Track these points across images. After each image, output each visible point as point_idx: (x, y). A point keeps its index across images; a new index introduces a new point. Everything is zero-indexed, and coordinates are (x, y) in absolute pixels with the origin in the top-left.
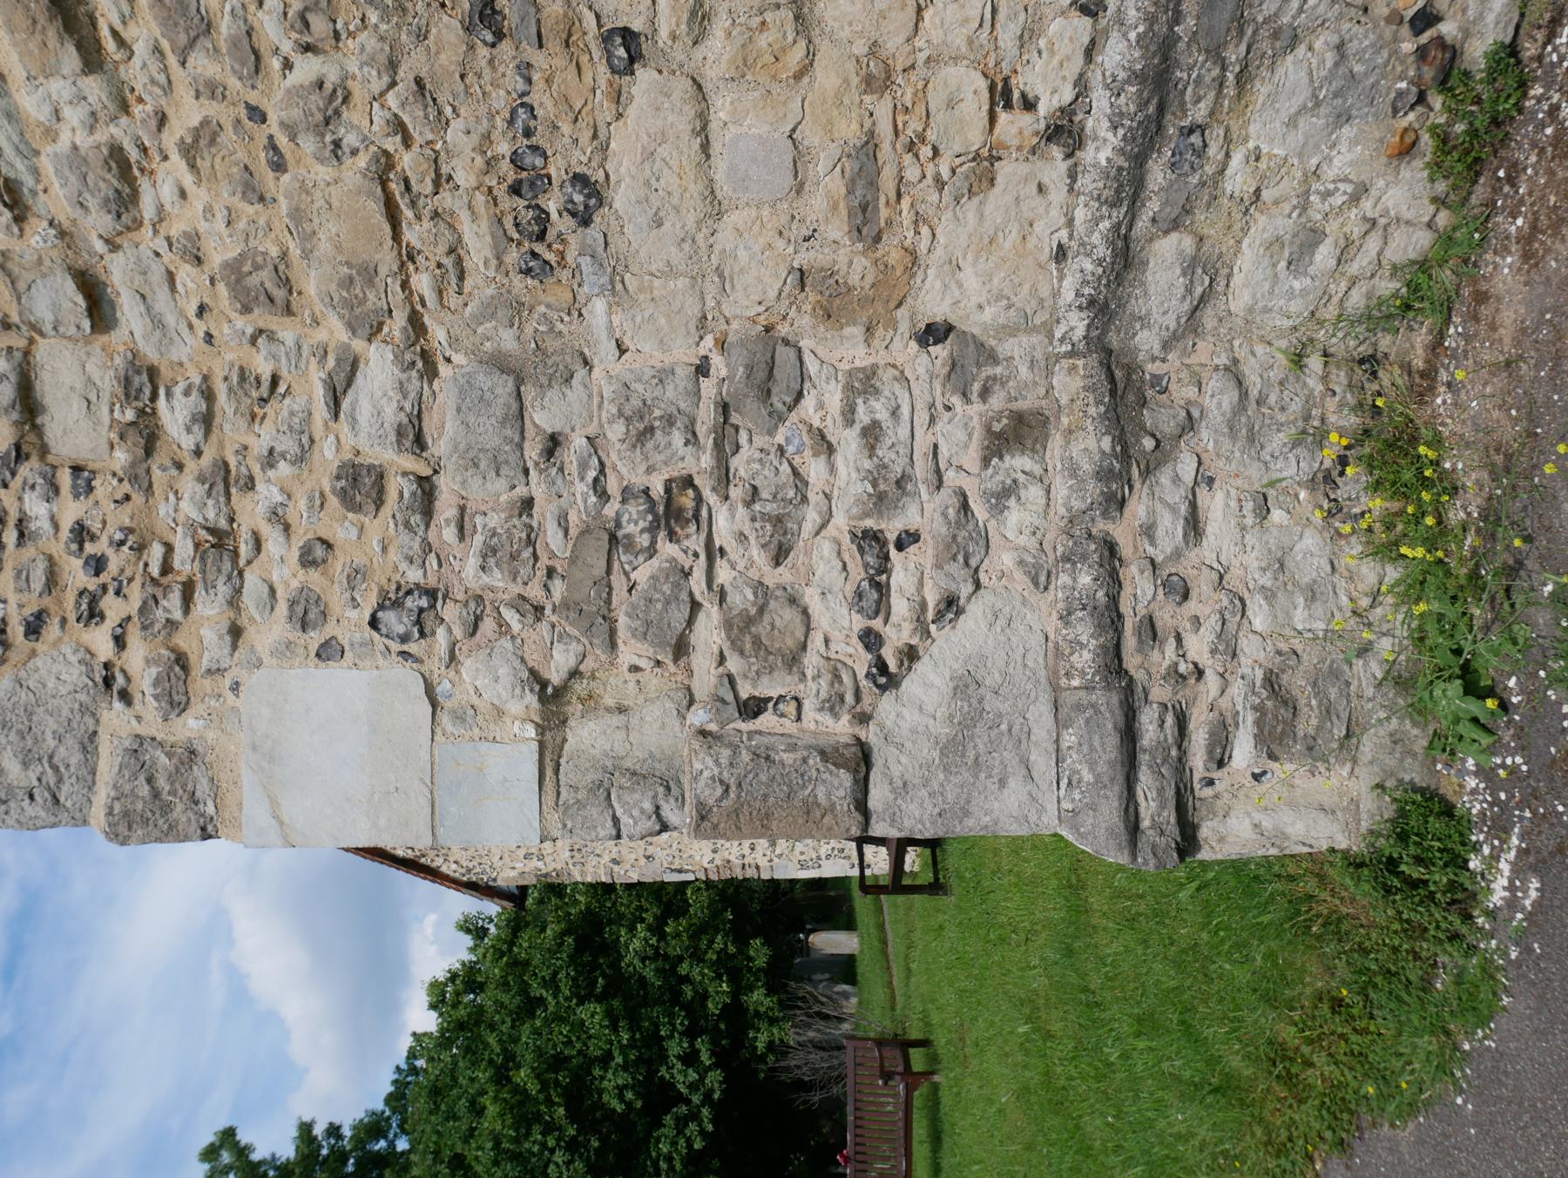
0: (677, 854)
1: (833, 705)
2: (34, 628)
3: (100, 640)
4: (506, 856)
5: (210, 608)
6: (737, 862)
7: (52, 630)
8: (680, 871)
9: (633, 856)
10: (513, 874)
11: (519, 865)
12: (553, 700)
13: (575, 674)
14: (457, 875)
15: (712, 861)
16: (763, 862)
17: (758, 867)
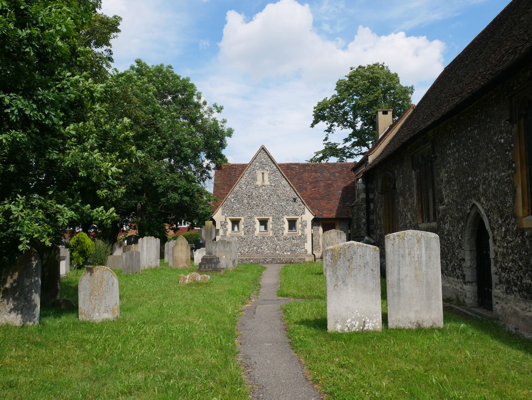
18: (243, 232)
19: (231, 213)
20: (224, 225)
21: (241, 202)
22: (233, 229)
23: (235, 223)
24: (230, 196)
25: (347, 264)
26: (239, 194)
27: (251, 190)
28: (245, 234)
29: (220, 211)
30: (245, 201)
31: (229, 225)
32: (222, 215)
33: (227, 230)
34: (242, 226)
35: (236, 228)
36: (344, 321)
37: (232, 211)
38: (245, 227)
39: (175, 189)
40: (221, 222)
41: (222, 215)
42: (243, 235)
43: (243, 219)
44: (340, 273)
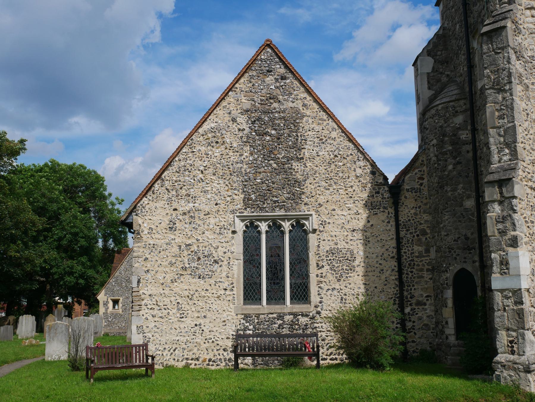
0: (149, 281)
1: (532, 326)
2: (528, 227)
3: (528, 235)
4: (151, 221)
5: (530, 248)
6: (143, 303)
7: (528, 229)
8: (139, 282)
9: (148, 266)
10: (140, 222)
11: (145, 225)
12: (528, 290)
13: (530, 293)
14: (141, 202)
15: (144, 294)
16: (141, 313)
17: (139, 311)
18: (121, 310)
19: (112, 294)
20: (106, 304)
21: (120, 285)
22: (114, 307)
23: (116, 302)
24: (112, 280)
25: (55, 331)
26: (119, 278)
27: (129, 276)
28: (122, 311)
29: (103, 292)
30: (124, 284)
31: (111, 304)
32: (105, 295)
33: (108, 308)
34: (120, 305)
35: (116, 307)
36: (52, 356)
37: (113, 292)
38: (123, 306)
39: (71, 274)
40: (104, 302)
41: (105, 295)
42: (121, 312)
43: (121, 299)
44: (52, 335)
